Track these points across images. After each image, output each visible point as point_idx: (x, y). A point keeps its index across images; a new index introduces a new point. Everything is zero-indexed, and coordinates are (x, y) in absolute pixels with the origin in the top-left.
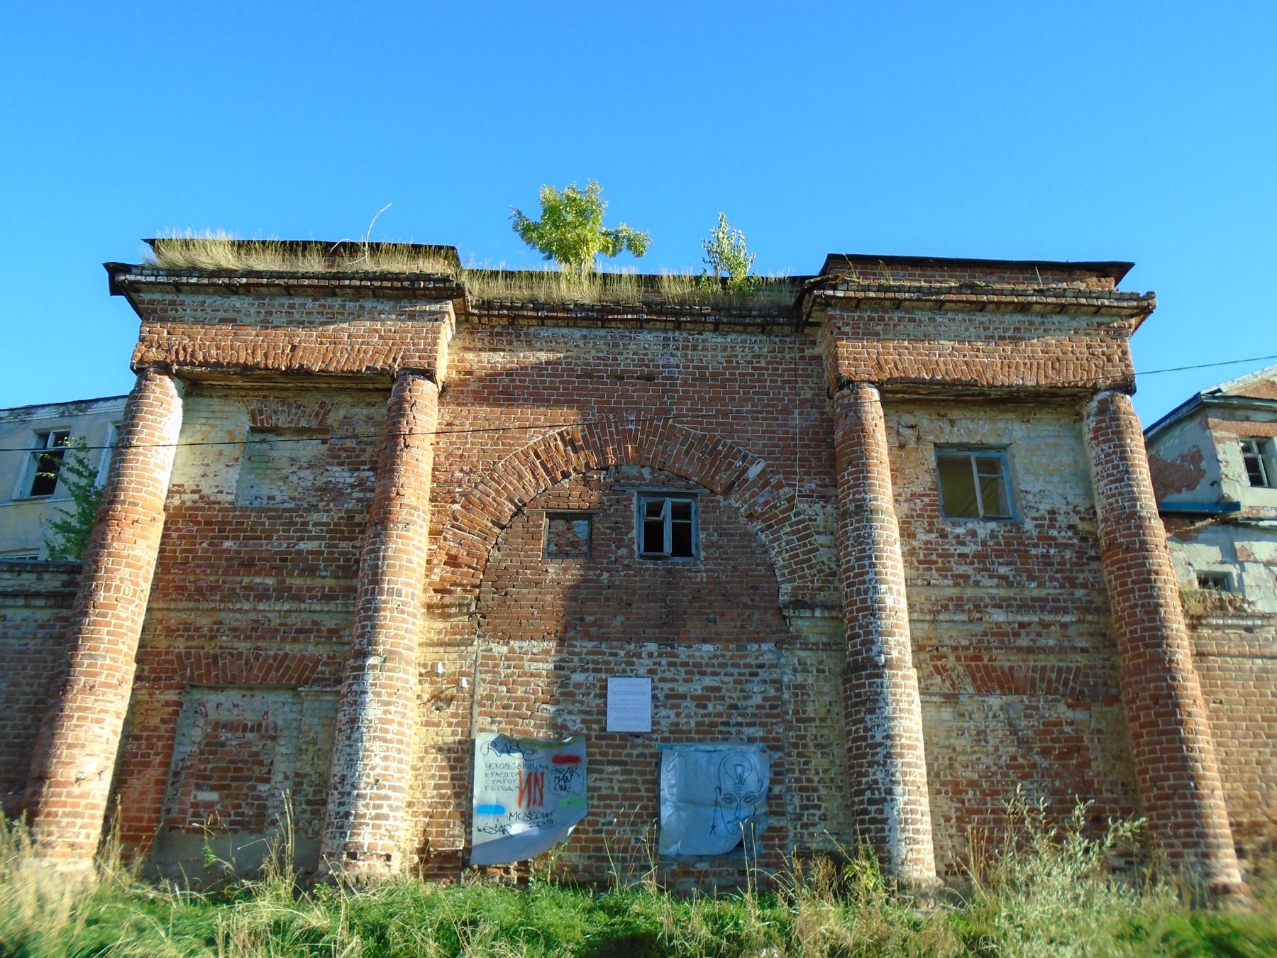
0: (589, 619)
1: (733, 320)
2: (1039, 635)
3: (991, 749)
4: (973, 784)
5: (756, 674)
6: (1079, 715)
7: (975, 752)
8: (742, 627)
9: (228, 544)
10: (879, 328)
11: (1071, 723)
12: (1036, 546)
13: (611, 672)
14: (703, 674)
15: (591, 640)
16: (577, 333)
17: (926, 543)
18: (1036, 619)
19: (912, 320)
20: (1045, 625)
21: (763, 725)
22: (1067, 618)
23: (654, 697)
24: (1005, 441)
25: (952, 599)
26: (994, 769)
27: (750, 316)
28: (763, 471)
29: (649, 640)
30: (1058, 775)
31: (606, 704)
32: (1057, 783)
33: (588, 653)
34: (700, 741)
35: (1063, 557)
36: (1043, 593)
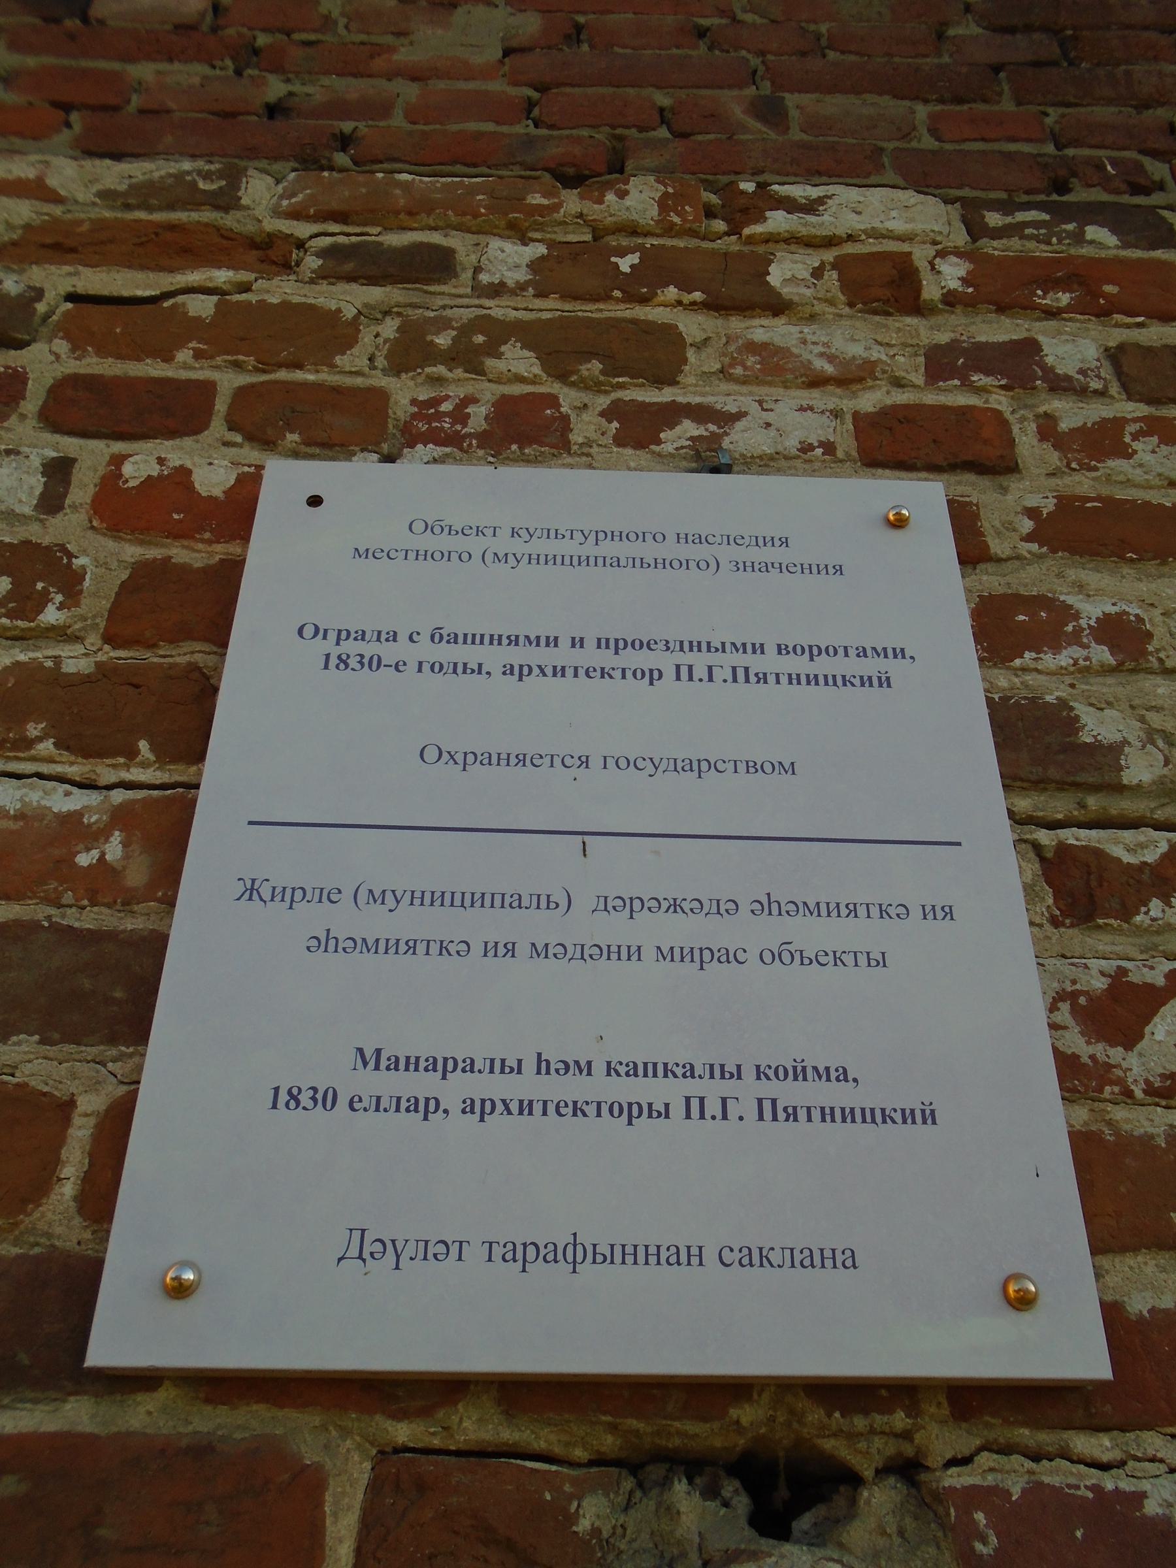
13: (349, 426)
15: (92, 148)
31: (166, 829)
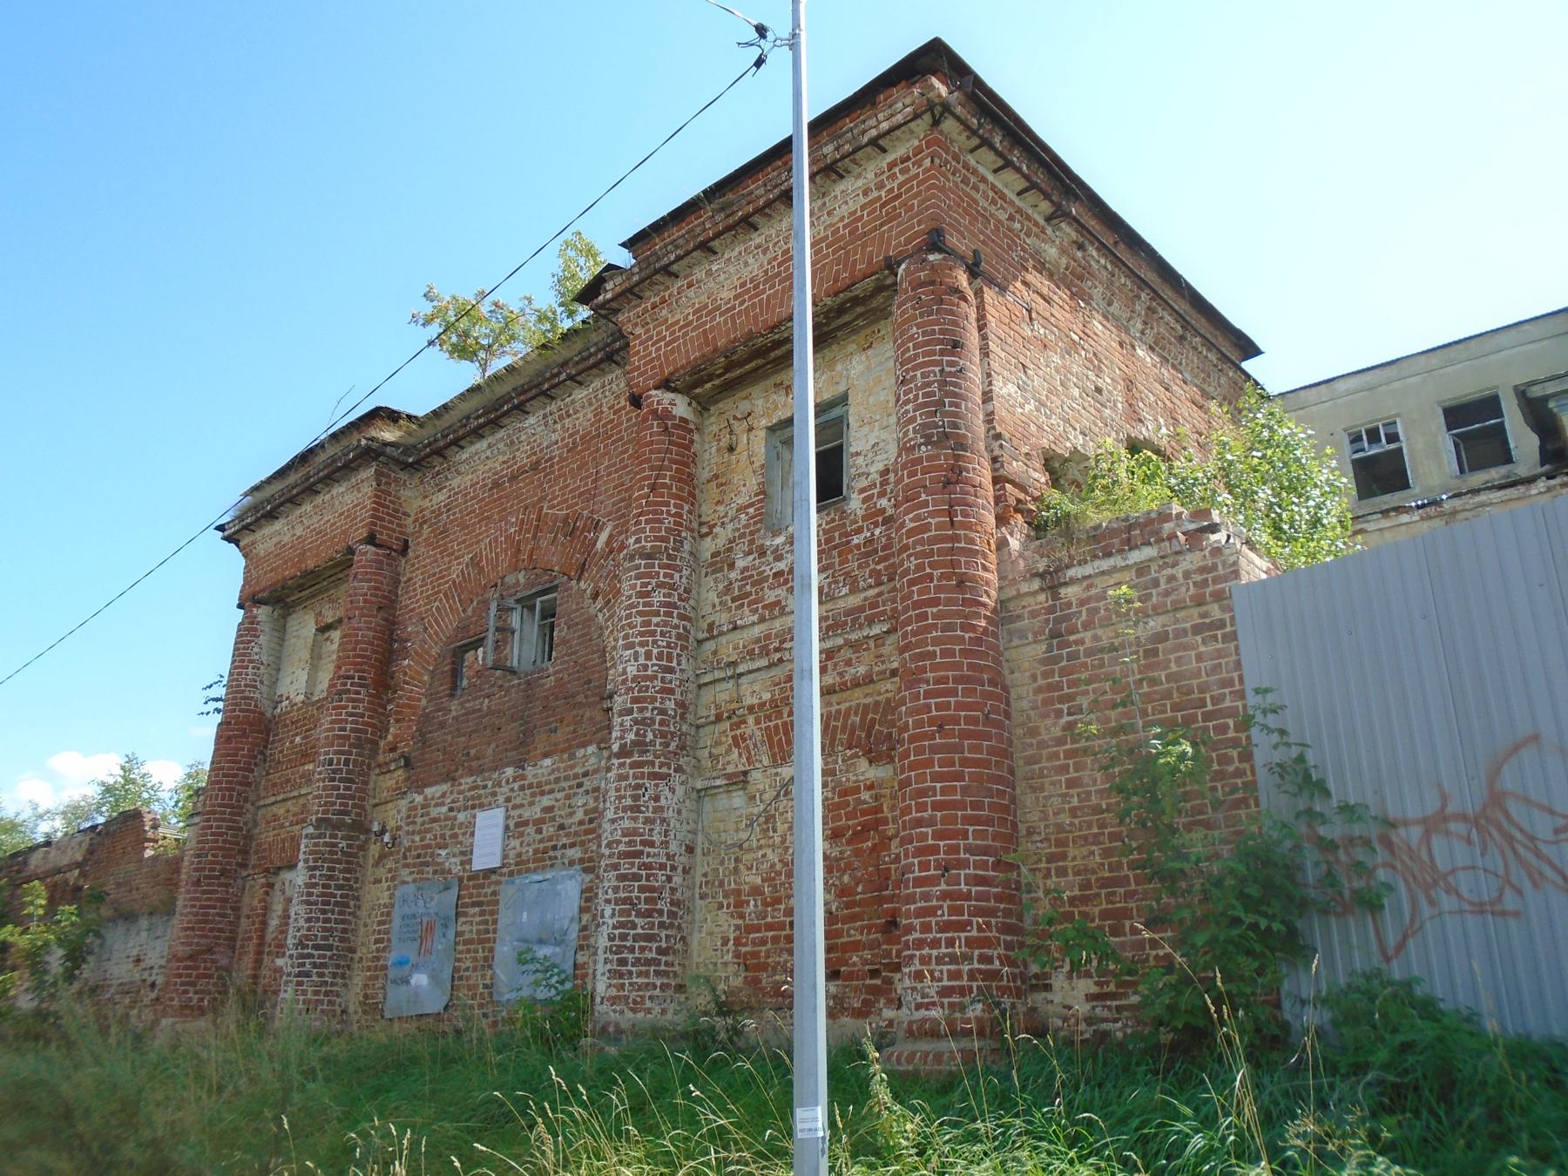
0: (473, 752)
1: (581, 367)
2: (849, 663)
3: (778, 840)
4: (756, 891)
5: (580, 785)
6: (881, 772)
7: (761, 847)
8: (575, 731)
9: (298, 739)
10: (664, 312)
11: (870, 787)
12: (859, 531)
13: (481, 806)
14: (542, 793)
16: (482, 445)
17: (746, 569)
18: (840, 641)
19: (690, 286)
20: (855, 646)
21: (582, 843)
22: (877, 630)
23: (507, 828)
24: (842, 389)
25: (758, 640)
26: (779, 867)
27: (591, 355)
28: (611, 536)
29: (508, 765)
30: (849, 867)
32: (846, 879)
33: (470, 789)
34: (535, 870)
35: (889, 538)
36: (855, 600)
